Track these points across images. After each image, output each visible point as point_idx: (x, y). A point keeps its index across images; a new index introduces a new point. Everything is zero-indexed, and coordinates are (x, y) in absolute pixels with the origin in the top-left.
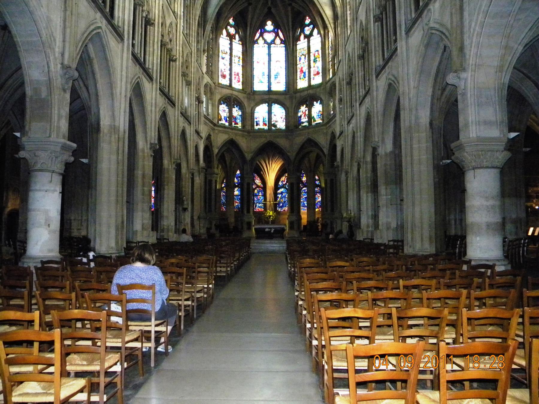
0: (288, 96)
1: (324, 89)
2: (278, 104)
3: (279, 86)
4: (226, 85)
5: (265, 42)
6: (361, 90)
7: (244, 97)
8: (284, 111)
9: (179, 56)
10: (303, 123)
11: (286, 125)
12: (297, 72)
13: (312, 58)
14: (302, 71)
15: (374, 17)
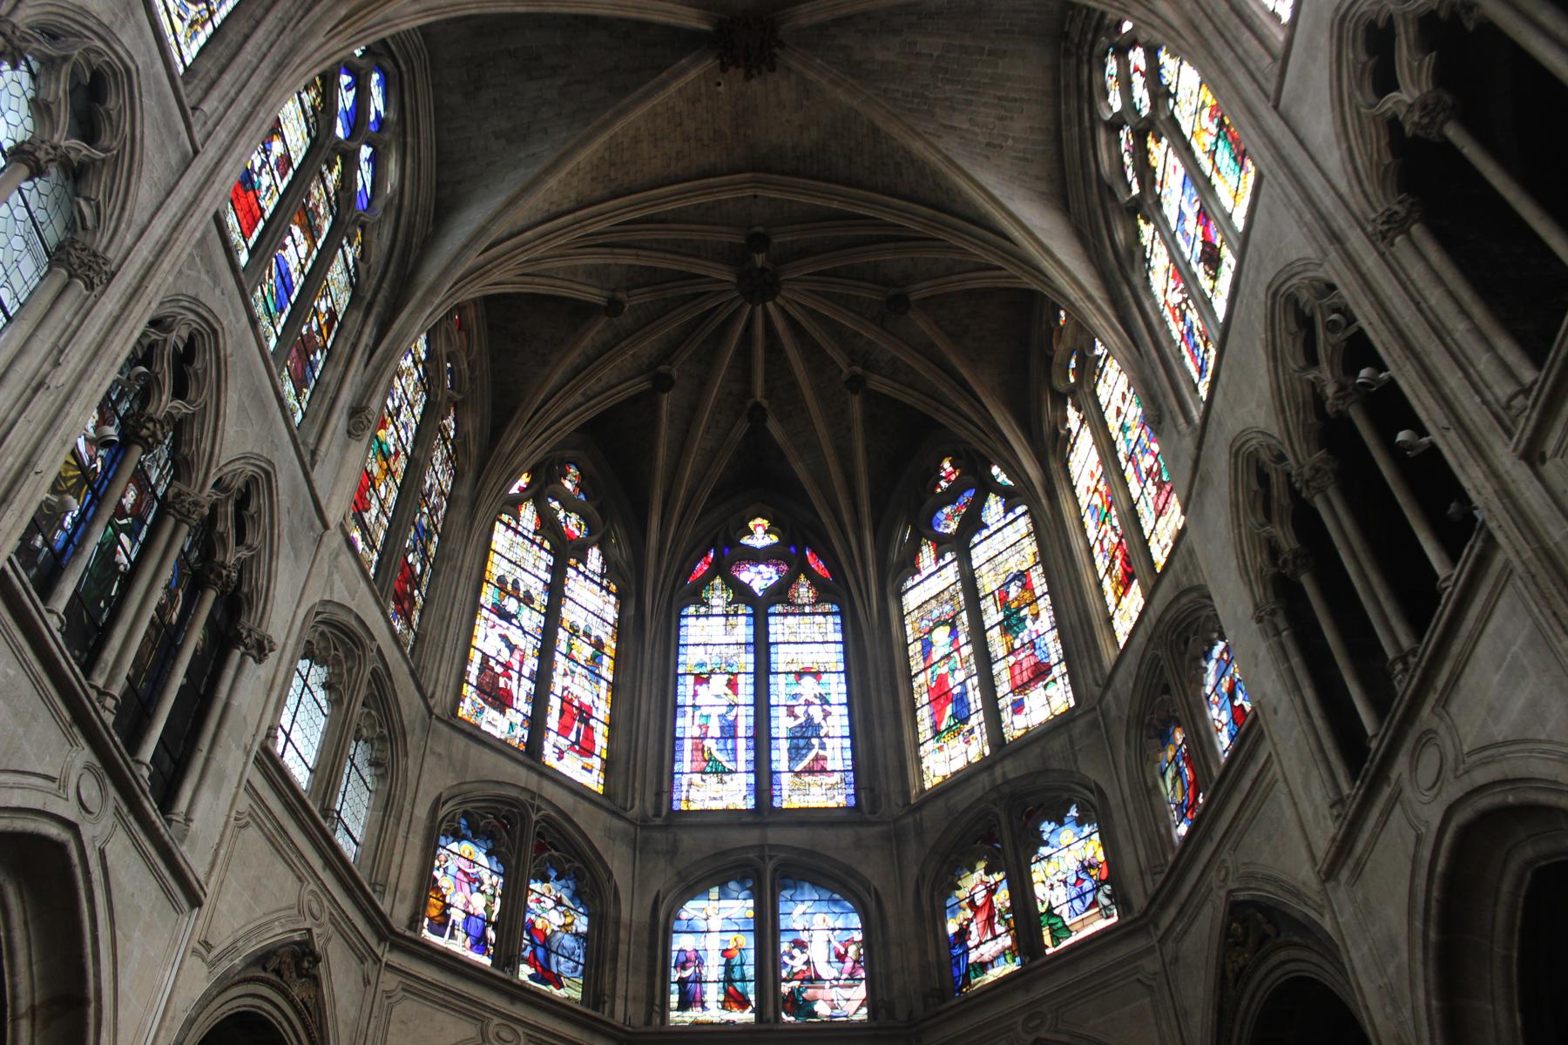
0: (875, 830)
1: (1094, 725)
2: (816, 884)
7: (610, 834)
8: (855, 921)
10: (983, 966)
11: (871, 1001)
12: (914, 710)
14: (940, 694)
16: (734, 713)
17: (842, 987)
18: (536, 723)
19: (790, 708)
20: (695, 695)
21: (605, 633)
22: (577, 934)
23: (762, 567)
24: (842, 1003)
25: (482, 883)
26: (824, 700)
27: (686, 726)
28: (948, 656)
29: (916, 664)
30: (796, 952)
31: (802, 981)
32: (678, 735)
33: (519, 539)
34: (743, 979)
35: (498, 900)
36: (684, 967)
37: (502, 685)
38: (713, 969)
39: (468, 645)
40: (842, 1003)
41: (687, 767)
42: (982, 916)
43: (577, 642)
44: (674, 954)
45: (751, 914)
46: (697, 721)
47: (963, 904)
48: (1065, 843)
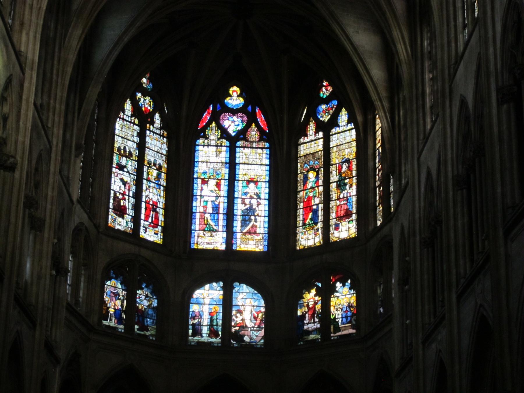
3: (253, 242)
4: (124, 233)
5: (224, 133)
6: (461, 262)
9: (22, 158)
12: (296, 209)
13: (334, 177)
14: (308, 207)
15: (498, 90)
16: (218, 201)
17: (255, 331)
18: (136, 219)
19: (243, 200)
20: (202, 190)
21: (162, 161)
22: (154, 308)
23: (235, 118)
24: (255, 337)
25: (119, 295)
26: (259, 197)
27: (197, 206)
28: (312, 188)
29: (300, 187)
30: (238, 315)
31: (240, 327)
32: (194, 211)
33: (125, 123)
34: (217, 325)
35: (125, 301)
36: (194, 319)
37: (122, 204)
38: (206, 321)
39: (109, 189)
40: (255, 337)
41: (197, 228)
42: (311, 312)
43: (150, 170)
44: (191, 313)
45: (221, 297)
46: (202, 205)
47: (305, 304)
48: (345, 293)
